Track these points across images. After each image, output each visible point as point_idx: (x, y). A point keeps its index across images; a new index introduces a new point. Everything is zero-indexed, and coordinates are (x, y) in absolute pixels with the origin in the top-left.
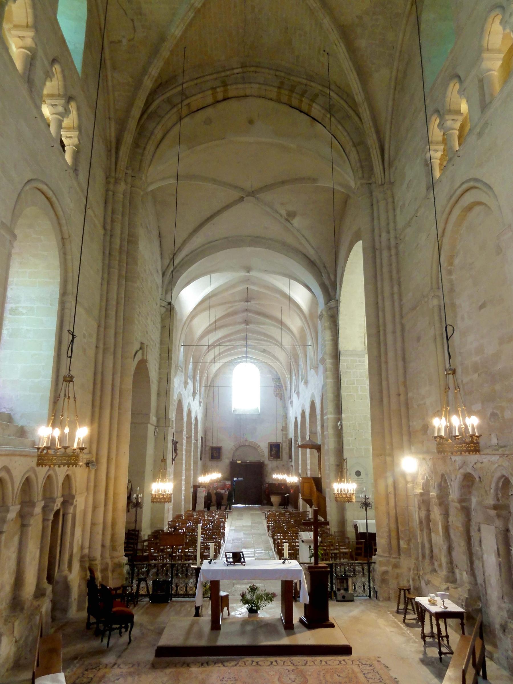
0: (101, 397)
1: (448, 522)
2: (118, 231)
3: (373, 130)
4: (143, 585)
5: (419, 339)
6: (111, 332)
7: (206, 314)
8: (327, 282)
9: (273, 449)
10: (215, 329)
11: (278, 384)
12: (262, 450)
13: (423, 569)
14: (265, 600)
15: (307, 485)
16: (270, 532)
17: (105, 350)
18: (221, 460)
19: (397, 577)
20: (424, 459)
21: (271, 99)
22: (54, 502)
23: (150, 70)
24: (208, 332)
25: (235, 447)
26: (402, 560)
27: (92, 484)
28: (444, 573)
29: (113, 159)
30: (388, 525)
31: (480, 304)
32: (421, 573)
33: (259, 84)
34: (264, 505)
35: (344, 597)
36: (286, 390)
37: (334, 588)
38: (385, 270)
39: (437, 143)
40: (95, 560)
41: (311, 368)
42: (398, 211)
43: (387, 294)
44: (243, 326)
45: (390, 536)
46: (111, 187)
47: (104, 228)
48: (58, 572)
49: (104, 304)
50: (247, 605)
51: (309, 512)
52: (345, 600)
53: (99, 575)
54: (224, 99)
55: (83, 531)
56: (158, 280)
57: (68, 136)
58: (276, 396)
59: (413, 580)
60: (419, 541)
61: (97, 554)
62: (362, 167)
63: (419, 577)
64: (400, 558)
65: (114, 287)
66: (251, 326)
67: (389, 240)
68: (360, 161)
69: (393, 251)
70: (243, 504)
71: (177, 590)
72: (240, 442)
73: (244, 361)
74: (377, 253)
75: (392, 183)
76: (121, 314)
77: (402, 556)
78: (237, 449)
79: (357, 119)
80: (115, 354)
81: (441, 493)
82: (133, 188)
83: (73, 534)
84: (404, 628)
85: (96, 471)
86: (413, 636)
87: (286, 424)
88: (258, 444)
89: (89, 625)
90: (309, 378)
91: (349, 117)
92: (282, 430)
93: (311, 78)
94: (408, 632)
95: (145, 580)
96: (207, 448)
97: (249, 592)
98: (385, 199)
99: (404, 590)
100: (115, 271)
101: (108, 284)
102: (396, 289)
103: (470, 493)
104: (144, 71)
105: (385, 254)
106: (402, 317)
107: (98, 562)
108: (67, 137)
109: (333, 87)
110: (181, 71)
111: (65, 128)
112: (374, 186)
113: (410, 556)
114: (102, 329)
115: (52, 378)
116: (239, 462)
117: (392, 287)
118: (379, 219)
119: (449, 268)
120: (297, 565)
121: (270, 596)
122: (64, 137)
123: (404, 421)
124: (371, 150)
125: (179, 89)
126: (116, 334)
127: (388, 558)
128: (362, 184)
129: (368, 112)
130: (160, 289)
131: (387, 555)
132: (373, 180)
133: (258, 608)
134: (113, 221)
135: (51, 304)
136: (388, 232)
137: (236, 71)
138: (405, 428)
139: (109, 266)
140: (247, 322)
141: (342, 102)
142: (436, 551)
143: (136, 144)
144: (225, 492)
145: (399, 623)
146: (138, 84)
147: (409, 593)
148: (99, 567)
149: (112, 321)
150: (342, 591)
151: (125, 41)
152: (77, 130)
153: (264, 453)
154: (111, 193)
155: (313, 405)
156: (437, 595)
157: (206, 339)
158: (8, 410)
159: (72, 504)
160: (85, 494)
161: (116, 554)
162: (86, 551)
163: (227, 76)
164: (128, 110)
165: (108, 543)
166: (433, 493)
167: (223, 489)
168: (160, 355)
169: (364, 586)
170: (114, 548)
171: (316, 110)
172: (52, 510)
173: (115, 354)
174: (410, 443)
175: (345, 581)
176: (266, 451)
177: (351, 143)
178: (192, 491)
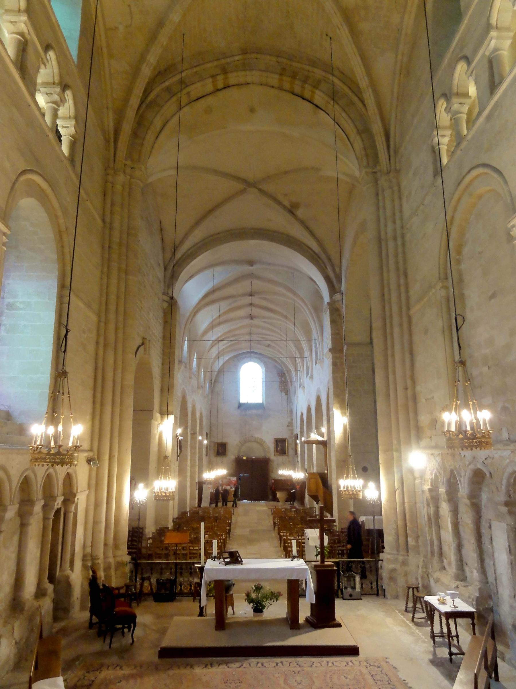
0: (102, 392)
1: (457, 519)
2: (117, 224)
3: (378, 117)
4: (146, 584)
5: (426, 331)
6: (112, 326)
7: (210, 308)
8: (331, 275)
10: (219, 324)
12: (268, 445)
13: (432, 566)
14: (271, 599)
15: (313, 481)
16: (276, 528)
17: (106, 346)
18: (227, 456)
19: (406, 574)
20: (432, 454)
21: (273, 87)
22: (55, 501)
23: (148, 57)
24: (212, 327)
26: (410, 557)
27: (93, 482)
28: (452, 570)
29: (112, 150)
30: (396, 522)
31: (490, 293)
32: (430, 571)
33: (261, 70)
35: (351, 595)
37: (341, 586)
38: (392, 261)
39: (445, 128)
40: (99, 559)
41: (316, 363)
42: (404, 200)
43: (393, 286)
44: (247, 321)
45: (397, 534)
46: (110, 178)
47: (104, 221)
48: (59, 571)
49: (104, 298)
50: (252, 604)
51: (315, 508)
52: (353, 598)
53: (101, 574)
54: (224, 88)
55: (85, 529)
56: (160, 274)
57: (64, 126)
59: (422, 578)
60: (428, 538)
61: (100, 552)
62: (367, 155)
63: (428, 575)
64: (408, 556)
65: (114, 281)
66: (255, 322)
67: (395, 230)
68: (365, 149)
69: (399, 242)
70: (248, 500)
71: (181, 589)
74: (383, 244)
75: (398, 171)
76: (121, 308)
77: (411, 553)
79: (360, 105)
80: (115, 349)
81: (450, 488)
82: (132, 180)
83: (74, 533)
84: (413, 627)
85: (98, 468)
86: (422, 636)
87: (292, 420)
89: (91, 625)
90: (315, 373)
91: (353, 103)
92: (288, 426)
93: (313, 63)
94: (417, 631)
95: (149, 579)
97: (254, 591)
98: (391, 188)
99: (413, 588)
100: (115, 265)
101: (108, 277)
102: (402, 281)
103: (480, 489)
104: (142, 58)
105: (391, 244)
106: (408, 309)
107: (100, 561)
108: (63, 127)
109: (336, 73)
110: (180, 58)
111: (61, 118)
112: (379, 174)
113: (419, 554)
114: (102, 325)
115: (51, 374)
116: (245, 458)
117: (398, 278)
118: (384, 208)
119: (457, 257)
120: (302, 563)
121: (275, 595)
122: (60, 127)
123: (411, 415)
124: (376, 137)
125: (178, 77)
126: (116, 328)
127: (396, 556)
128: (367, 173)
129: (372, 97)
130: (162, 283)
131: (395, 552)
132: (378, 168)
133: (264, 607)
134: (112, 213)
135: (49, 299)
136: (394, 222)
137: (236, 58)
138: (412, 423)
139: (109, 260)
140: (251, 317)
141: (346, 89)
142: (445, 548)
143: (135, 134)
144: (231, 488)
145: (408, 622)
146: (136, 71)
147: (418, 591)
148: (102, 566)
149: (112, 316)
150: (349, 590)
151: (121, 28)
152: (74, 120)
154: (109, 185)
155: (318, 400)
156: (447, 594)
157: (210, 333)
158: (7, 407)
159: (74, 502)
160: (87, 492)
161: (119, 553)
162: (89, 550)
163: (228, 63)
164: (126, 100)
165: (111, 541)
166: (442, 490)
168: (163, 351)
169: (371, 584)
170: (116, 546)
171: (319, 98)
172: (53, 508)
173: (115, 349)
174: (419, 437)
175: (352, 579)
176: (271, 446)
177: (355, 131)
178: (197, 488)
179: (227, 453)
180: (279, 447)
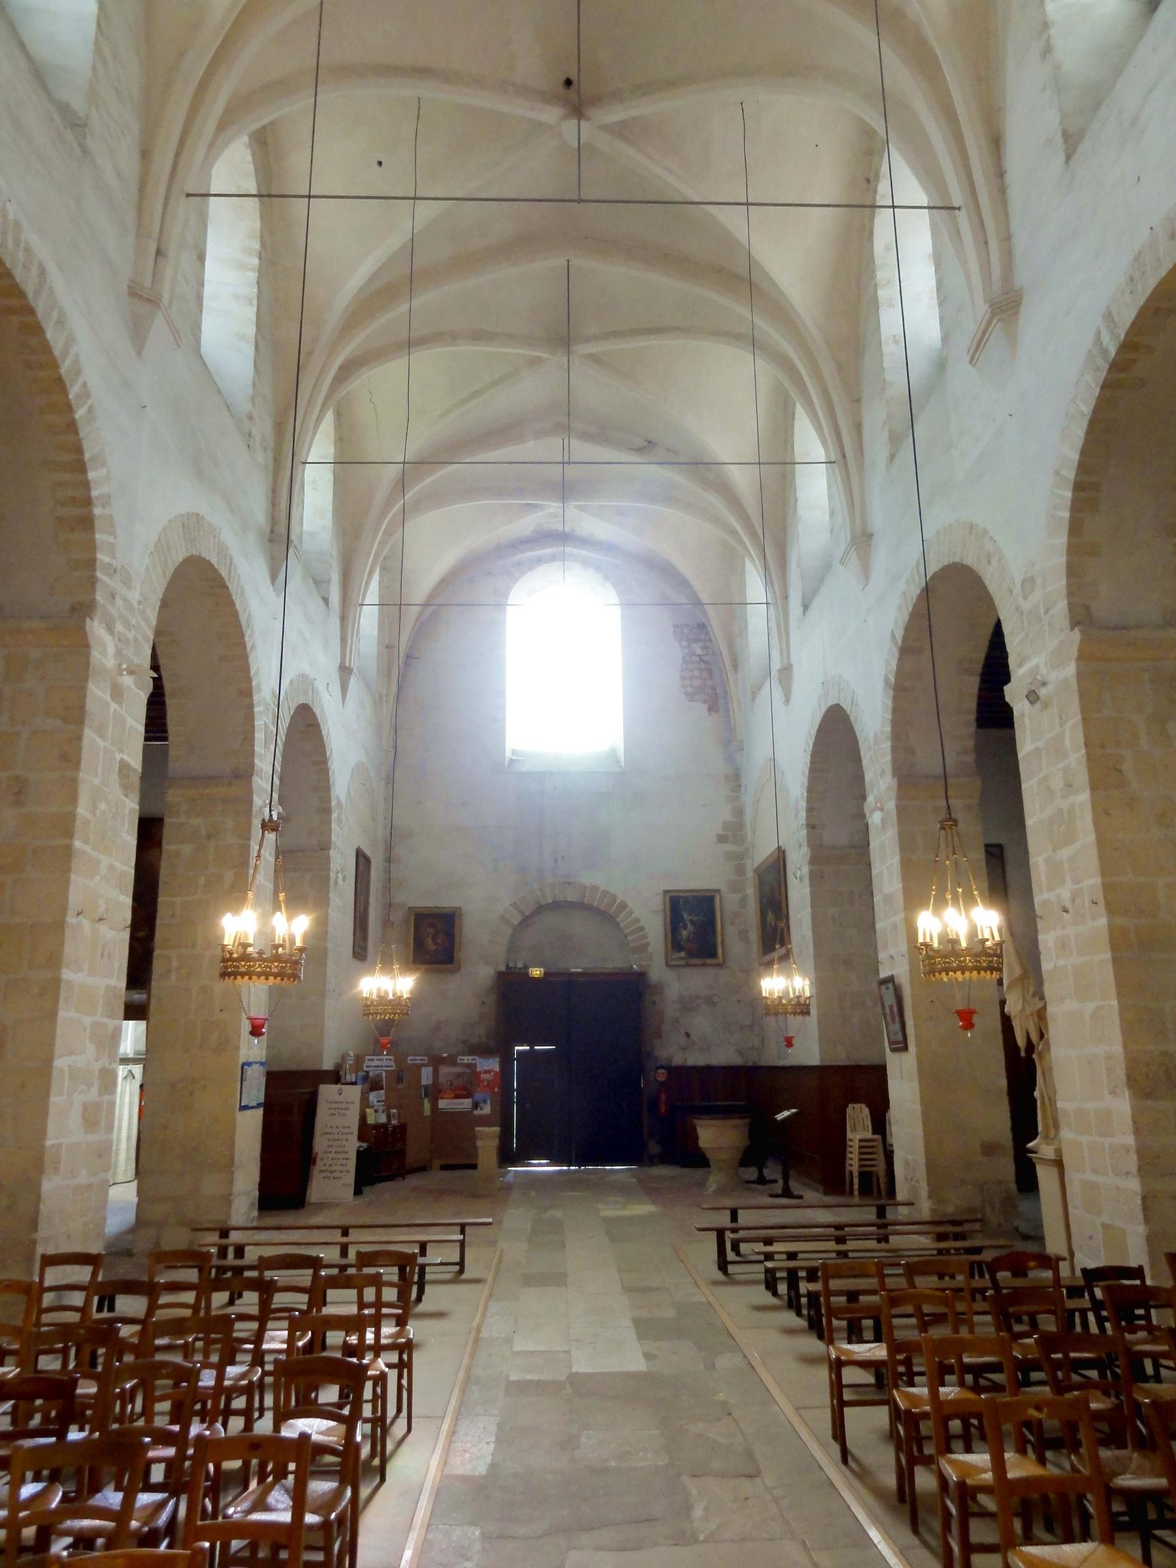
9: (686, 916)
12: (637, 920)
18: (459, 969)
25: (522, 913)
34: (652, 1161)
36: (735, 667)
58: (691, 697)
70: (555, 1161)
73: (553, 558)
78: (526, 921)
87: (739, 812)
92: (722, 839)
96: (397, 916)
116: (536, 972)
144: (476, 1106)
153: (645, 936)
167: (463, 1092)
180: (685, 928)
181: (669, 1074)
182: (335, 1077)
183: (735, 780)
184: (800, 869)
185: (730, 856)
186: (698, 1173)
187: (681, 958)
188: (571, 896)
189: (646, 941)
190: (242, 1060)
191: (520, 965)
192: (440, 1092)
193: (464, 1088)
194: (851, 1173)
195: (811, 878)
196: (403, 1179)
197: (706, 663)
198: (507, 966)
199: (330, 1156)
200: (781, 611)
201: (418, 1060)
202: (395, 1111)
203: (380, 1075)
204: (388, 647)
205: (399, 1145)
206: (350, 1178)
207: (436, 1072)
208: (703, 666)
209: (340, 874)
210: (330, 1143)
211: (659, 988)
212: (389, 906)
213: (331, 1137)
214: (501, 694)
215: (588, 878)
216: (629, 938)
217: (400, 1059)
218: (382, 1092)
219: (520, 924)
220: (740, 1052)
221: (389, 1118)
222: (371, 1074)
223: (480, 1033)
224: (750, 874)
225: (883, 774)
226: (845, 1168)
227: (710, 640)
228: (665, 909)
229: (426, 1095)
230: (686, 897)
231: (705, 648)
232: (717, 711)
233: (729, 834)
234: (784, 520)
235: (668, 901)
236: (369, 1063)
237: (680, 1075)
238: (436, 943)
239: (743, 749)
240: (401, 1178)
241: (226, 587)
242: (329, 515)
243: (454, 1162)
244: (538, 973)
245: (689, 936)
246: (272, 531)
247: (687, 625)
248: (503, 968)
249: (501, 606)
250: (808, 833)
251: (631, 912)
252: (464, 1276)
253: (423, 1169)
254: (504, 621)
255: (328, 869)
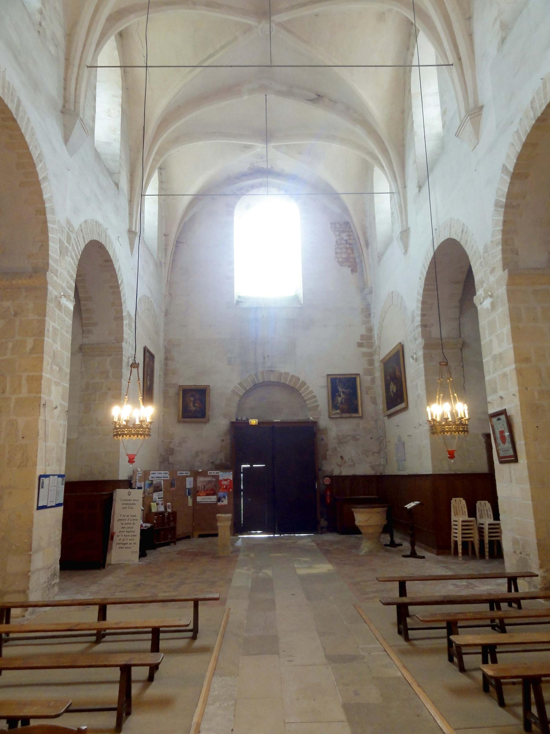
11: (345, 236)
12: (311, 392)
18: (208, 420)
36: (367, 245)
58: (341, 264)
70: (265, 531)
72: (256, 375)
73: (261, 185)
78: (247, 393)
87: (370, 330)
88: (302, 378)
92: (360, 345)
96: (172, 392)
116: (253, 422)
144: (219, 500)
153: (316, 401)
179: (208, 413)
180: (340, 396)
181: (331, 479)
182: (128, 484)
183: (367, 312)
184: (415, 353)
185: (365, 354)
186: (352, 539)
187: (338, 413)
188: (273, 378)
189: (316, 404)
190: (38, 473)
191: (244, 419)
192: (198, 492)
193: (212, 490)
194: (456, 542)
195: (424, 358)
196: (175, 544)
197: (350, 244)
198: (237, 419)
199: (124, 534)
200: (402, 197)
201: (184, 473)
202: (169, 504)
203: (160, 483)
204: (164, 235)
205: (172, 524)
206: (137, 548)
207: (195, 481)
208: (348, 246)
209: (130, 359)
210: (123, 526)
211: (325, 431)
212: (167, 386)
213: (124, 522)
214: (231, 263)
215: (283, 368)
216: (307, 402)
217: (173, 473)
218: (162, 492)
219: (244, 395)
220: (373, 468)
221: (166, 508)
222: (154, 482)
223: (221, 458)
224: (378, 365)
225: (493, 270)
226: (451, 538)
227: (352, 231)
228: (328, 386)
229: (189, 494)
230: (340, 378)
231: (349, 236)
232: (356, 272)
233: (365, 342)
234: (403, 140)
235: (329, 380)
236: (153, 475)
237: (338, 480)
238: (194, 406)
239: (372, 293)
240: (173, 544)
241: (14, 120)
242: (119, 132)
243: (207, 533)
244: (255, 422)
245: (342, 401)
246: (64, 106)
247: (338, 223)
248: (234, 420)
249: (231, 213)
250: (423, 331)
251: (308, 387)
252: (198, 643)
253: (188, 537)
254: (232, 222)
255: (122, 355)
